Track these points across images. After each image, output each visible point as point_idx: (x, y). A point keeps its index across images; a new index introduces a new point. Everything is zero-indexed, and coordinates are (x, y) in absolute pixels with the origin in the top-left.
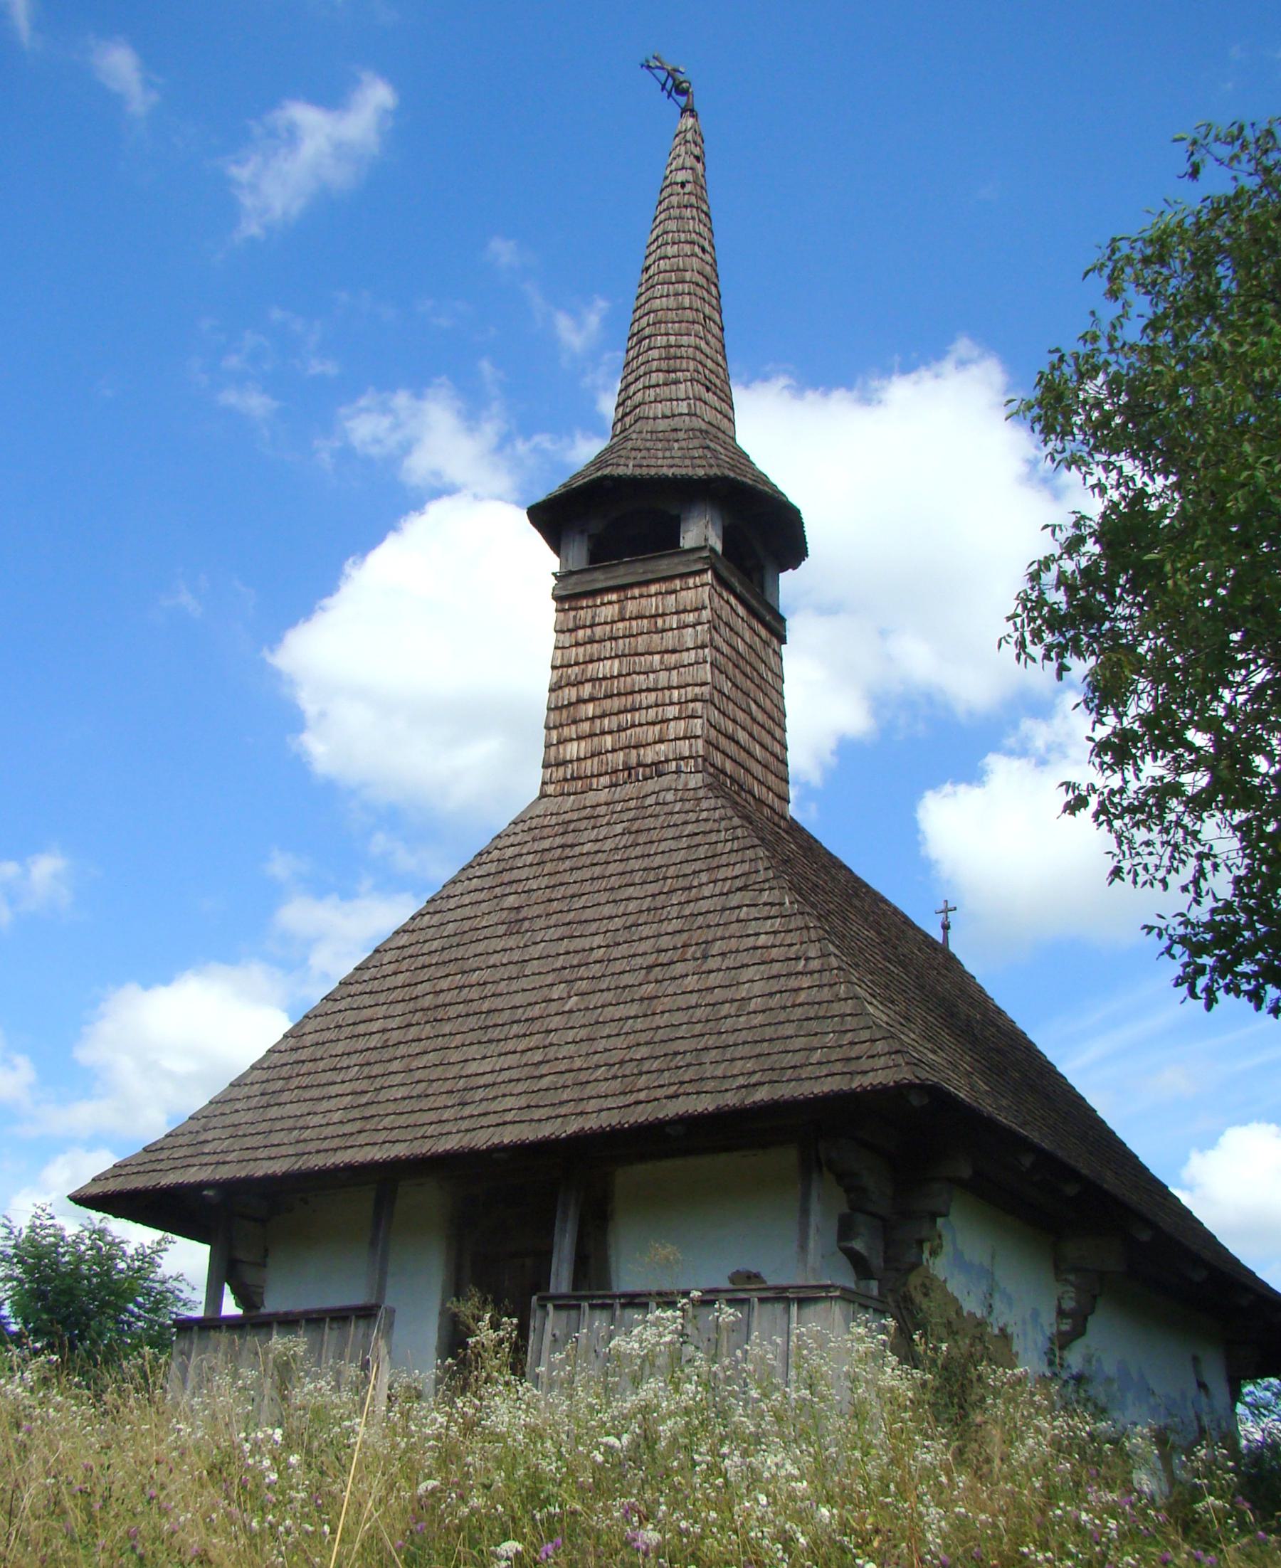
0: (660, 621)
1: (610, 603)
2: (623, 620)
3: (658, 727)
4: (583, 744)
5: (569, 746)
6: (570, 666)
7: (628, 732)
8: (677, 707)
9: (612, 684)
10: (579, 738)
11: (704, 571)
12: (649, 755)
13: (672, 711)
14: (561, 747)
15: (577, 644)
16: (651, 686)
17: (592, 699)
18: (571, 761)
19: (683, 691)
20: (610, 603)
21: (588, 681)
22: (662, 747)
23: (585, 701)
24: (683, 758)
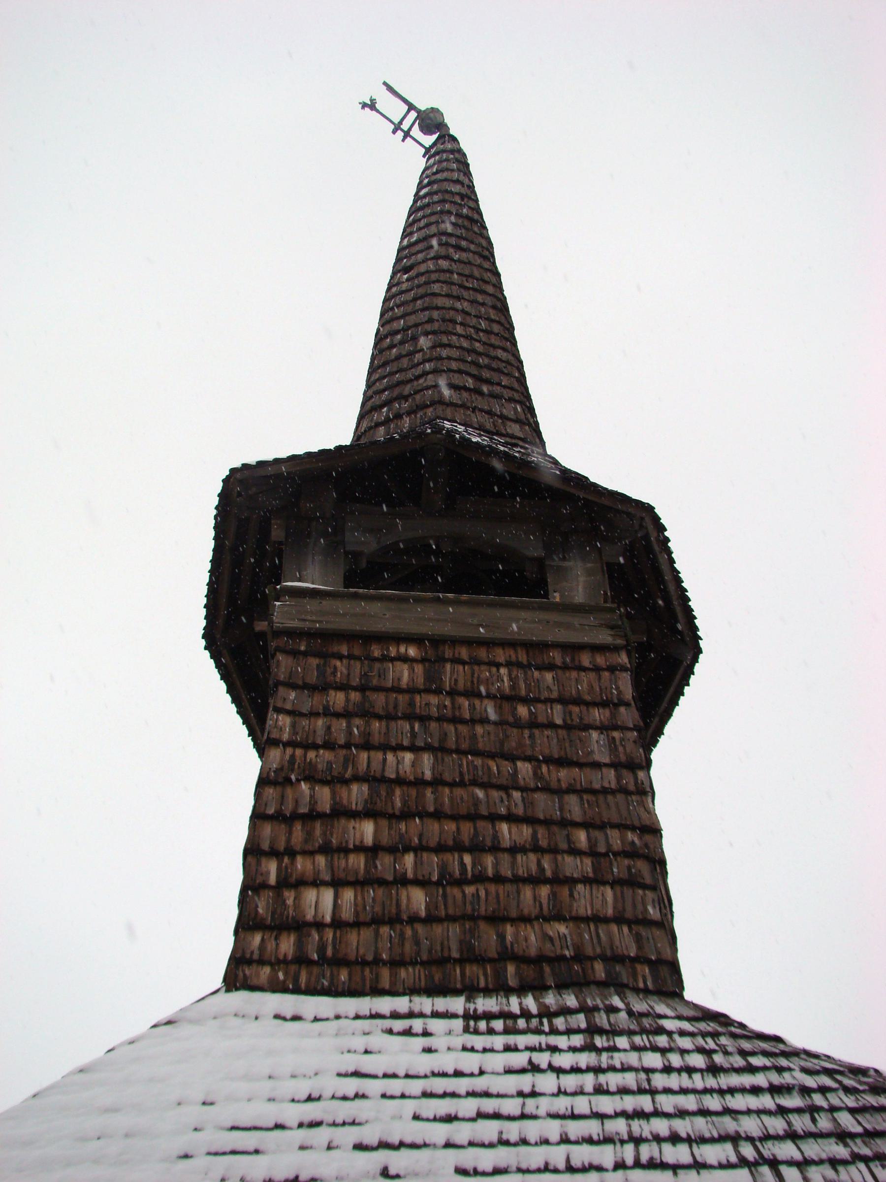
0: (523, 711)
1: (405, 659)
2: (438, 692)
3: (544, 891)
4: (348, 895)
5: (310, 895)
6: (316, 747)
7: (469, 890)
8: (588, 861)
9: (421, 796)
10: (337, 884)
11: (616, 649)
12: (531, 939)
14: (289, 896)
15: (328, 712)
16: (520, 811)
17: (369, 813)
18: (319, 925)
19: (597, 834)
20: (405, 659)
21: (357, 778)
22: (562, 929)
23: (354, 815)
24: (620, 959)
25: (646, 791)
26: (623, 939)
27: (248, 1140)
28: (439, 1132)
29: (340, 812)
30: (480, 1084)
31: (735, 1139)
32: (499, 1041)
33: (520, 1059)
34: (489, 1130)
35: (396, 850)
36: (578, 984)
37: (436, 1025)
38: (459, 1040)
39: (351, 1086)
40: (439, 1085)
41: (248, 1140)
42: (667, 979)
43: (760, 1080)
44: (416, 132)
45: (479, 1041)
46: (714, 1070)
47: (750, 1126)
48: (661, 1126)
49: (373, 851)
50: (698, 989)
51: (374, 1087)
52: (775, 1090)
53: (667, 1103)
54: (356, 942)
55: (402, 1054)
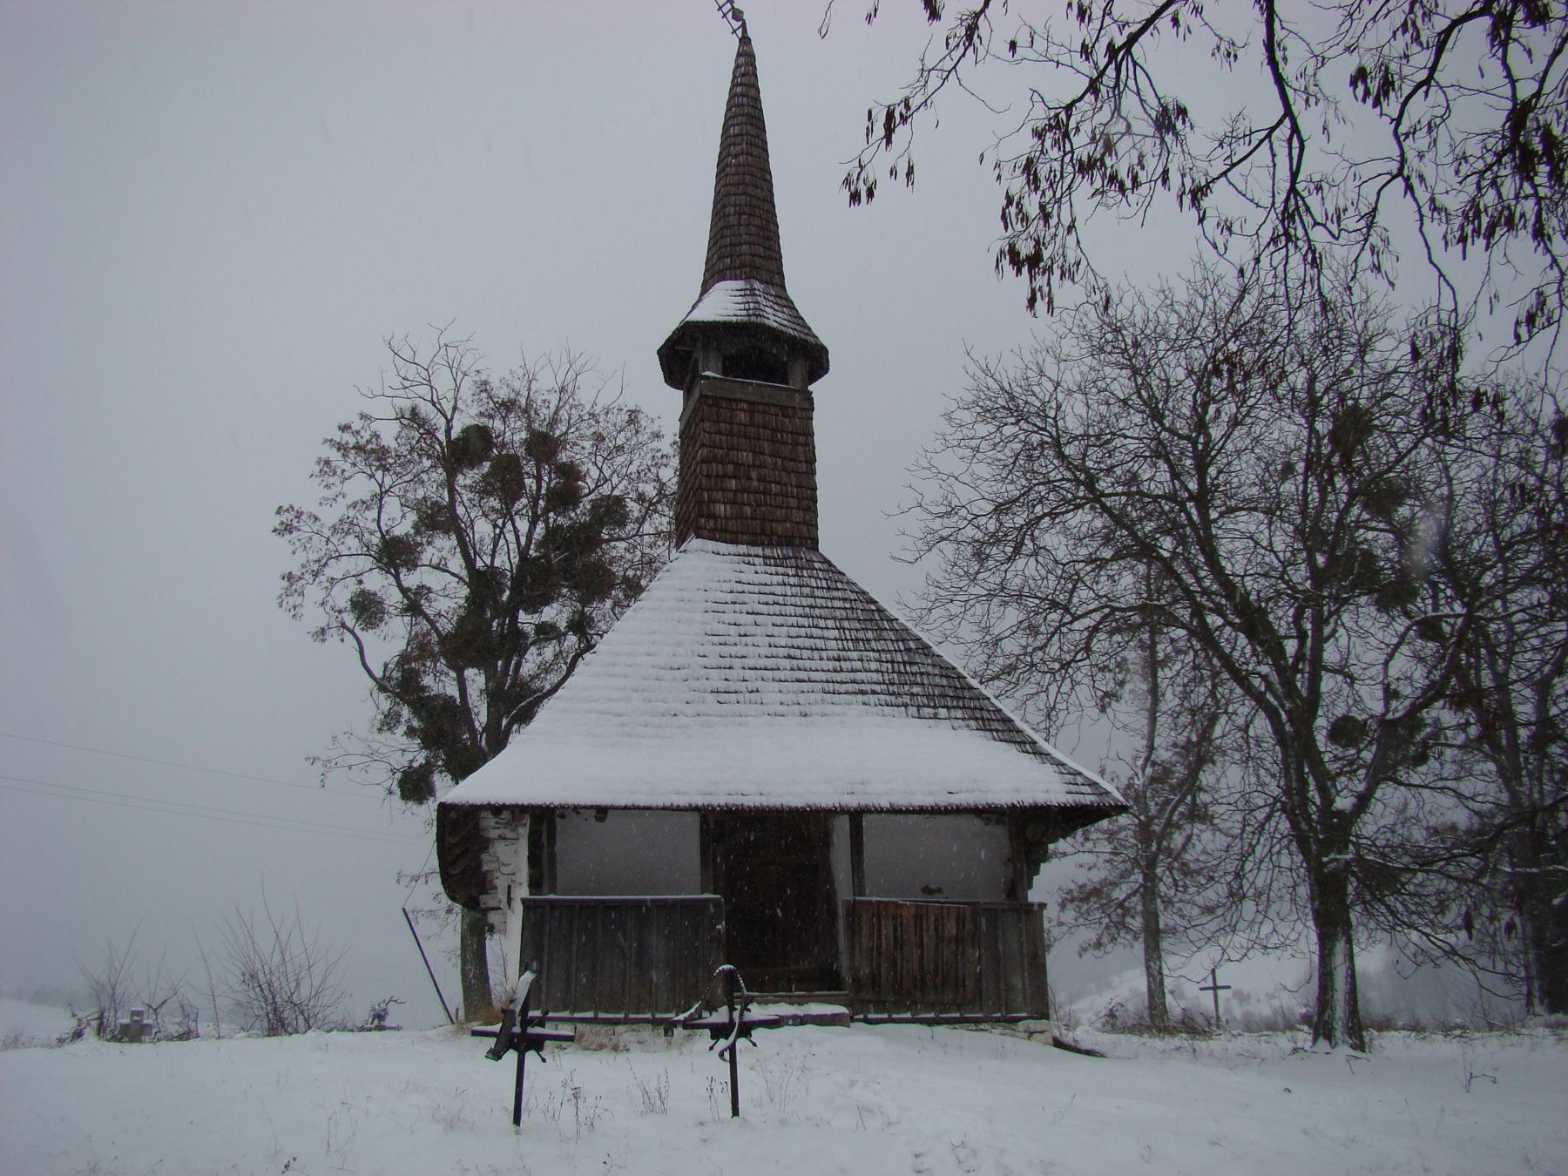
13: (793, 502)
15: (720, 433)
25: (813, 473)
26: (804, 529)
27: (720, 607)
28: (765, 609)
29: (725, 476)
30: (773, 589)
31: (834, 619)
32: (773, 569)
33: (780, 579)
34: (776, 609)
35: (743, 491)
36: (790, 544)
37: (757, 560)
38: (764, 568)
39: (740, 587)
40: (763, 589)
41: (720, 607)
42: (814, 546)
43: (839, 594)
44: (730, 15)
45: (768, 569)
46: (829, 588)
47: (838, 613)
48: (817, 612)
49: (735, 492)
50: (823, 548)
51: (746, 588)
52: (845, 600)
53: (820, 602)
54: (732, 524)
55: (749, 574)
